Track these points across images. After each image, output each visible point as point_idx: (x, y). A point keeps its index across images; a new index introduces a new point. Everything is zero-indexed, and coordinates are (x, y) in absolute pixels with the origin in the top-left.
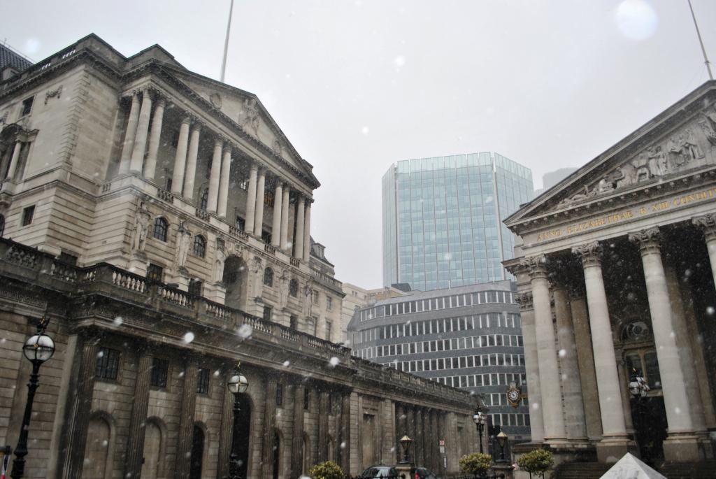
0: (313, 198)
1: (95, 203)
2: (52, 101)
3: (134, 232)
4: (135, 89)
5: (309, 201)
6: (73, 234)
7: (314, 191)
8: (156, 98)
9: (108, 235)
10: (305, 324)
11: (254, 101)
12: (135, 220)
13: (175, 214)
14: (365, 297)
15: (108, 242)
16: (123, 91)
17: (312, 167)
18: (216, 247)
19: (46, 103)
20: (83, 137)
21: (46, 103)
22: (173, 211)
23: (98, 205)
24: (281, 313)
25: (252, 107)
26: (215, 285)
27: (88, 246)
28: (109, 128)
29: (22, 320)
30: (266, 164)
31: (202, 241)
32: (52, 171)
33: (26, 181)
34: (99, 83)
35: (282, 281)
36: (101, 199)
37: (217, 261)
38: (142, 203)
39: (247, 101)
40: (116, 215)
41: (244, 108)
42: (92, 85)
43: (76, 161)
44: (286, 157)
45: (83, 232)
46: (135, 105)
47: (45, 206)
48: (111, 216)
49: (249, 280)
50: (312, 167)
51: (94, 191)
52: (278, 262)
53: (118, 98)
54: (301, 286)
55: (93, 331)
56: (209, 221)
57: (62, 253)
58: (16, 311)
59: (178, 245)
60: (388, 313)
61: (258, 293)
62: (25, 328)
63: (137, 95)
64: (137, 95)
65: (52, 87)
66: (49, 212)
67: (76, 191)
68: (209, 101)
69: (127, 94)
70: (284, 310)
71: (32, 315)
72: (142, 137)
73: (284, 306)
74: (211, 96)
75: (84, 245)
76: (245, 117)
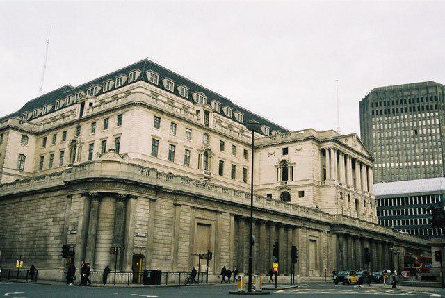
8: (334, 149)
22: (343, 189)
31: (349, 196)
47: (309, 192)
52: (366, 197)
55: (342, 233)
65: (298, 146)
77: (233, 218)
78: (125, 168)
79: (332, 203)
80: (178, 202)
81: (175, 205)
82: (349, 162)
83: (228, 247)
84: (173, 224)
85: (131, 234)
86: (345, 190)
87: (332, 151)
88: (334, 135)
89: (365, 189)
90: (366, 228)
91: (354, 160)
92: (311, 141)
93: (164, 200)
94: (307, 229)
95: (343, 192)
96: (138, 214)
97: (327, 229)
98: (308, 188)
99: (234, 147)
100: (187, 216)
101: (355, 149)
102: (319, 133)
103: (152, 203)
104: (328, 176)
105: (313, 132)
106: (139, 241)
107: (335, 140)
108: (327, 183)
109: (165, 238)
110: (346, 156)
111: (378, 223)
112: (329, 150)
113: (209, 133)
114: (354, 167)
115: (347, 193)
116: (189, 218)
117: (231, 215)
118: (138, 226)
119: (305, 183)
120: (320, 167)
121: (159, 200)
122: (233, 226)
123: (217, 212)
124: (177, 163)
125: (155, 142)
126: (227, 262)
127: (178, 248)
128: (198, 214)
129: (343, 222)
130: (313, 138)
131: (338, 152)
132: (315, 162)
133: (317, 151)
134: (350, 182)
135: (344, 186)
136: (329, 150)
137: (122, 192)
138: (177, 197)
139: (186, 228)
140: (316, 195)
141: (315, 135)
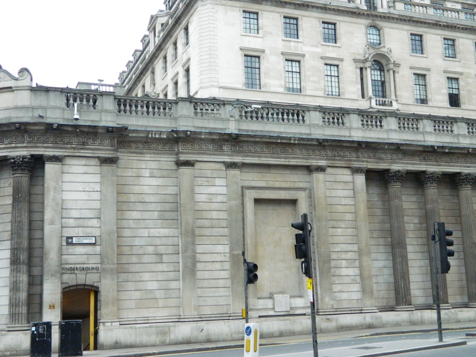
77: (361, 179)
78: (24, 98)
80: (183, 158)
81: (180, 164)
83: (355, 248)
84: (174, 210)
85: (51, 242)
93: (148, 157)
96: (66, 196)
99: (451, 44)
100: (214, 187)
103: (107, 168)
106: (77, 255)
109: (158, 241)
113: (381, 23)
116: (224, 190)
117: (356, 171)
118: (71, 222)
121: (125, 157)
122: (363, 196)
123: (309, 169)
124: (308, 92)
125: (252, 59)
126: (354, 282)
127: (195, 262)
128: (253, 178)
137: (20, 151)
138: (181, 148)
139: (214, 215)
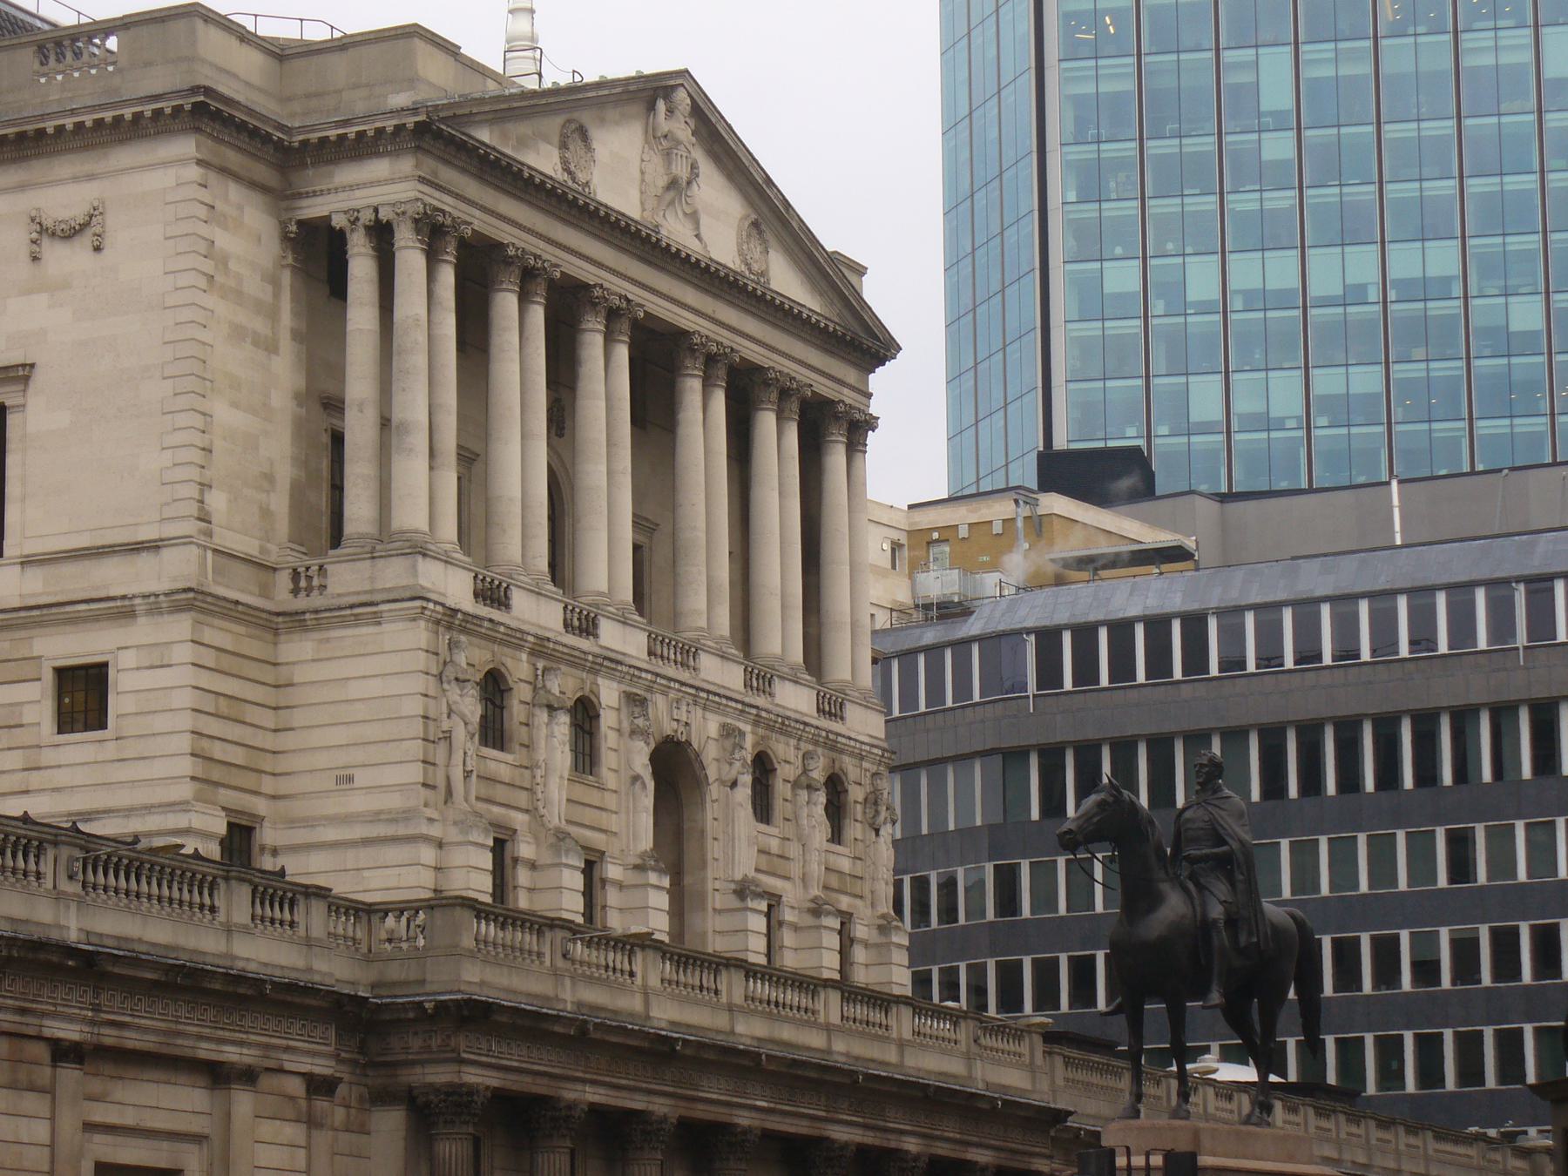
0: (874, 409)
1: (276, 632)
2: (64, 259)
3: (443, 746)
4: (363, 199)
5: (858, 428)
6: (237, 756)
7: (879, 380)
8: (433, 231)
9: (358, 756)
10: (877, 945)
11: (681, 96)
12: (445, 709)
13: (520, 647)
14: (896, 547)
15: (358, 782)
16: (300, 196)
17: (860, 271)
18: (626, 725)
19: (35, 258)
20: (224, 413)
21: (35, 258)
22: (514, 639)
23: (283, 638)
24: (809, 920)
25: (682, 129)
26: (636, 867)
27: (284, 786)
28: (272, 348)
29: (296, 1087)
30: (726, 337)
31: (585, 714)
32: (153, 546)
33: (27, 562)
34: (235, 192)
35: (803, 795)
36: (297, 621)
37: (636, 778)
38: (452, 645)
39: (661, 105)
40: (374, 688)
41: (653, 136)
42: (219, 205)
43: (217, 501)
44: (786, 281)
45: (268, 741)
46: (361, 268)
47: (157, 676)
48: (355, 690)
49: (709, 816)
50: (860, 271)
51: (265, 592)
52: (784, 725)
53: (283, 225)
54: (856, 794)
55: (458, 1099)
56: (596, 636)
57: (230, 825)
58: (288, 1066)
59: (541, 755)
60: (1049, 674)
61: (745, 864)
62: (303, 1103)
63: (367, 228)
64: (367, 228)
66: (185, 699)
67: (231, 610)
68: (561, 176)
69: (314, 209)
70: (817, 910)
71: (317, 1070)
72: (413, 406)
73: (815, 891)
74: (564, 146)
75: (268, 785)
76: (662, 181)
79: (394, 777)
82: (606, 374)
86: (541, 649)
87: (410, 259)
88: (438, 81)
89: (781, 635)
90: (749, 1030)
91: (658, 359)
92: (185, 146)
94: (64, 1053)
95: (519, 667)
97: (312, 1053)
98: (144, 630)
101: (675, 231)
102: (281, 53)
104: (359, 511)
105: (213, 43)
107: (440, 135)
108: (346, 578)
110: (567, 306)
111: (900, 979)
112: (382, 234)
114: (654, 415)
115: (564, 685)
119: (116, 577)
120: (282, 400)
129: (476, 978)
130: (205, 113)
131: (479, 269)
132: (232, 359)
133: (249, 237)
134: (605, 564)
135: (537, 612)
136: (382, 234)
140: (230, 709)
141: (242, 79)
